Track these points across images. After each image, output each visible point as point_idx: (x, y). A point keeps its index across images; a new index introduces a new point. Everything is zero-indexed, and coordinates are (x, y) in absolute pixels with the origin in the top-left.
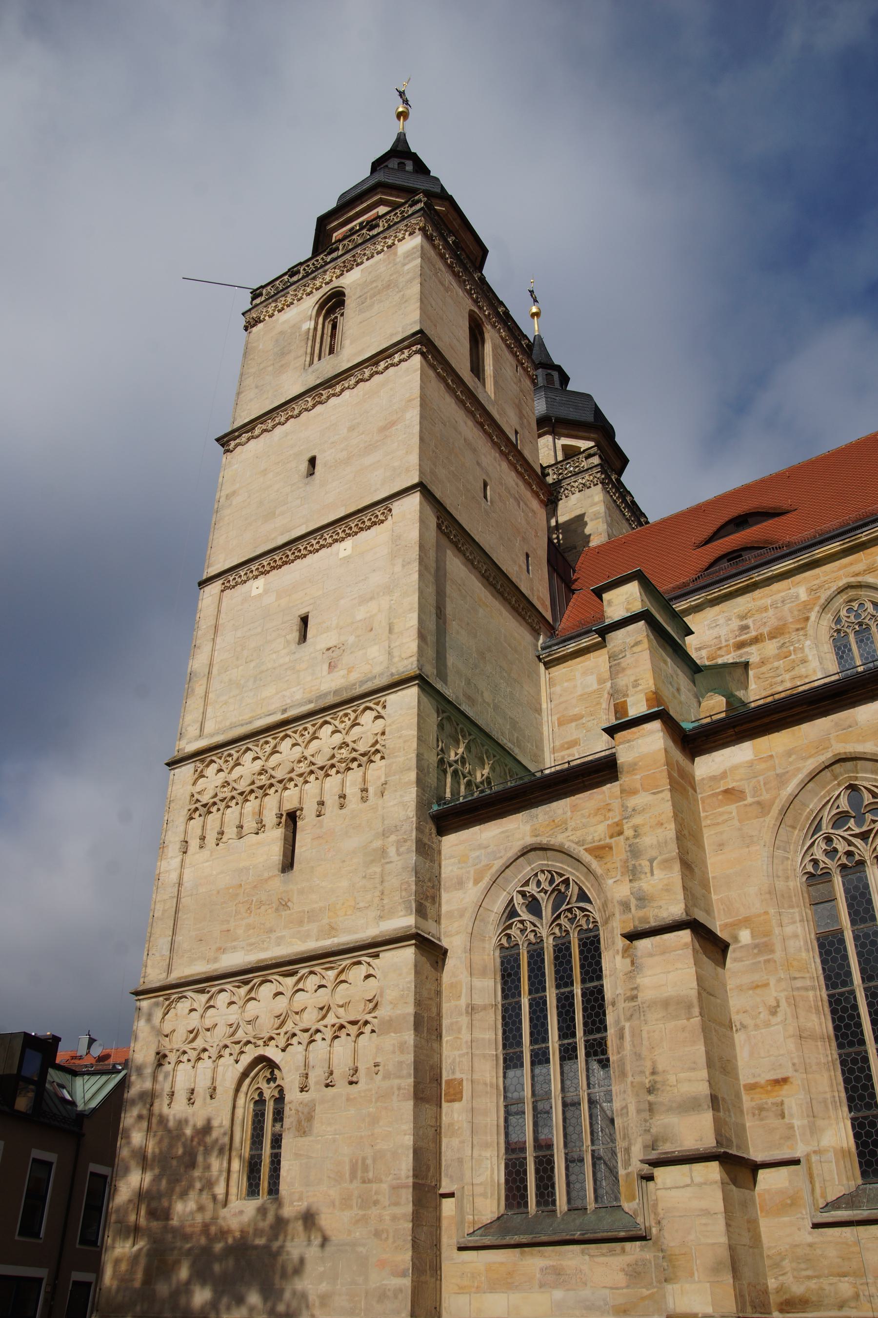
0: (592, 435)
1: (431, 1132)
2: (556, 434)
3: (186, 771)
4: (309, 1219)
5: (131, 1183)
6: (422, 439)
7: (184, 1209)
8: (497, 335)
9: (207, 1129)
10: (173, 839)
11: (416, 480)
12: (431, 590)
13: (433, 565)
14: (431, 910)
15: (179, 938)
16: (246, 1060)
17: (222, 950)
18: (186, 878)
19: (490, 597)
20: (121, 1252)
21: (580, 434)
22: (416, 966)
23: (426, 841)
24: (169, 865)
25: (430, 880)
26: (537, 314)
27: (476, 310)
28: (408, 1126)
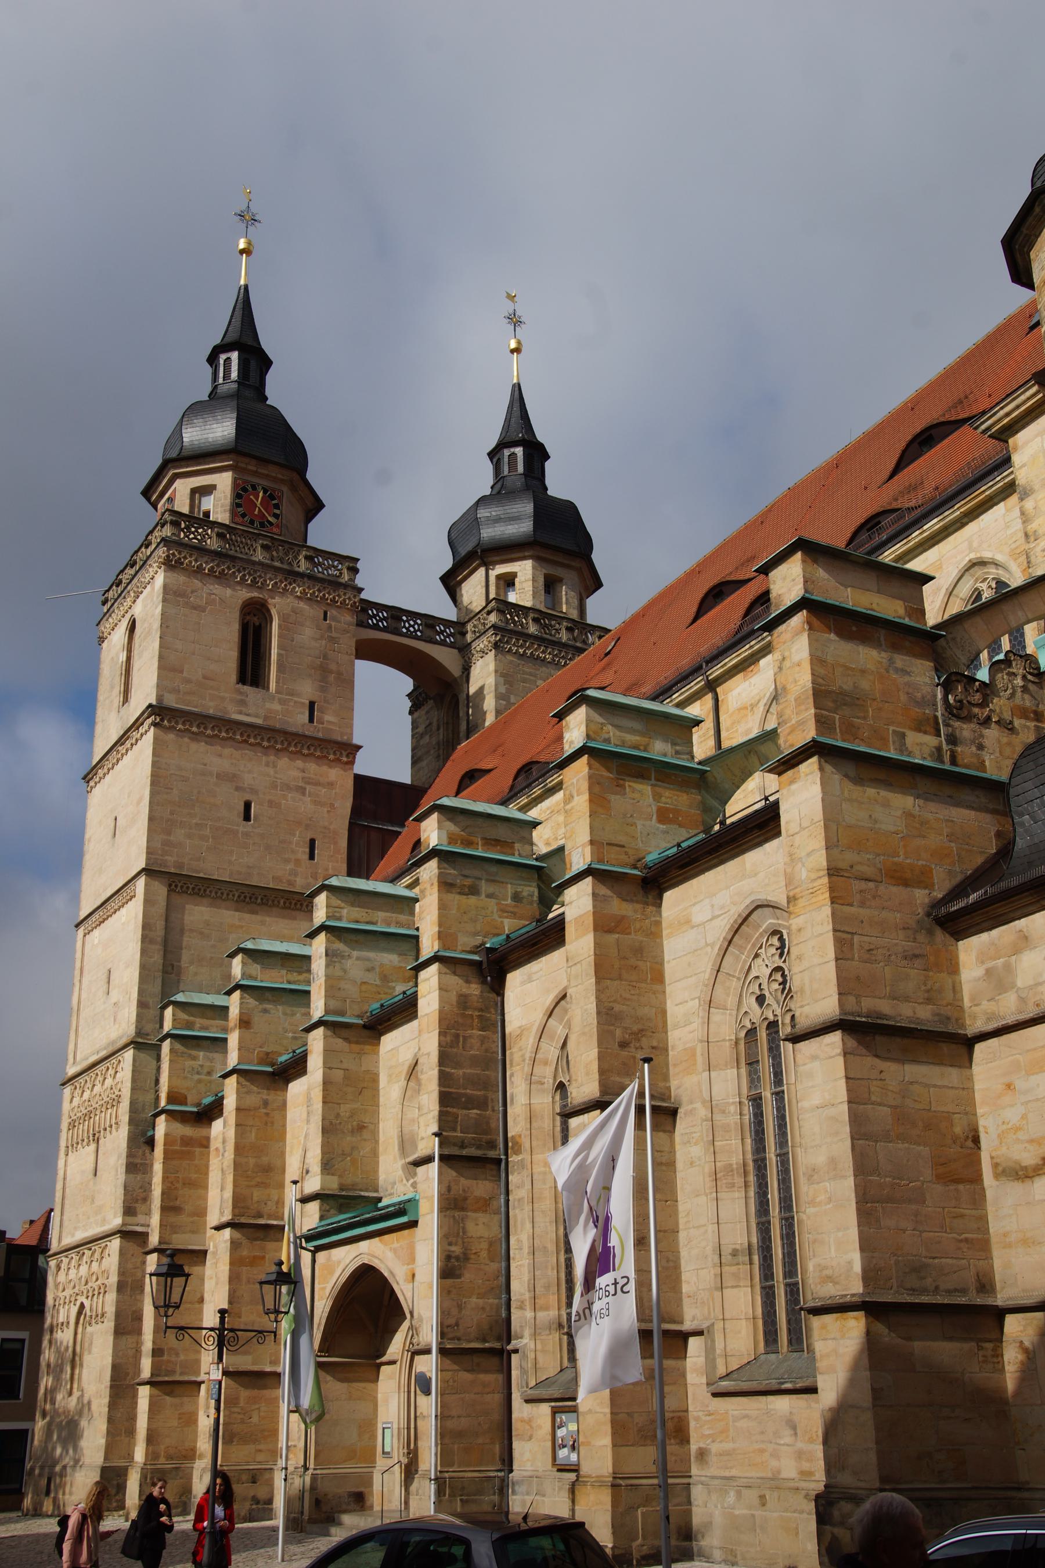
0: (527, 554)
1: (131, 1353)
2: (488, 565)
3: (67, 1091)
4: (89, 1403)
5: (46, 1381)
6: (151, 819)
7: (59, 1397)
8: (290, 599)
9: (67, 1348)
10: (63, 1144)
11: (142, 864)
12: (157, 958)
13: (159, 932)
14: (140, 1207)
15: (65, 1218)
16: (78, 1303)
17: (76, 1228)
18: (68, 1172)
19: (247, 916)
20: (40, 1424)
21: (513, 556)
22: (121, 1251)
23: (138, 1161)
24: (61, 1163)
25: (141, 1188)
26: (517, 350)
27: (256, 594)
28: (110, 1351)
